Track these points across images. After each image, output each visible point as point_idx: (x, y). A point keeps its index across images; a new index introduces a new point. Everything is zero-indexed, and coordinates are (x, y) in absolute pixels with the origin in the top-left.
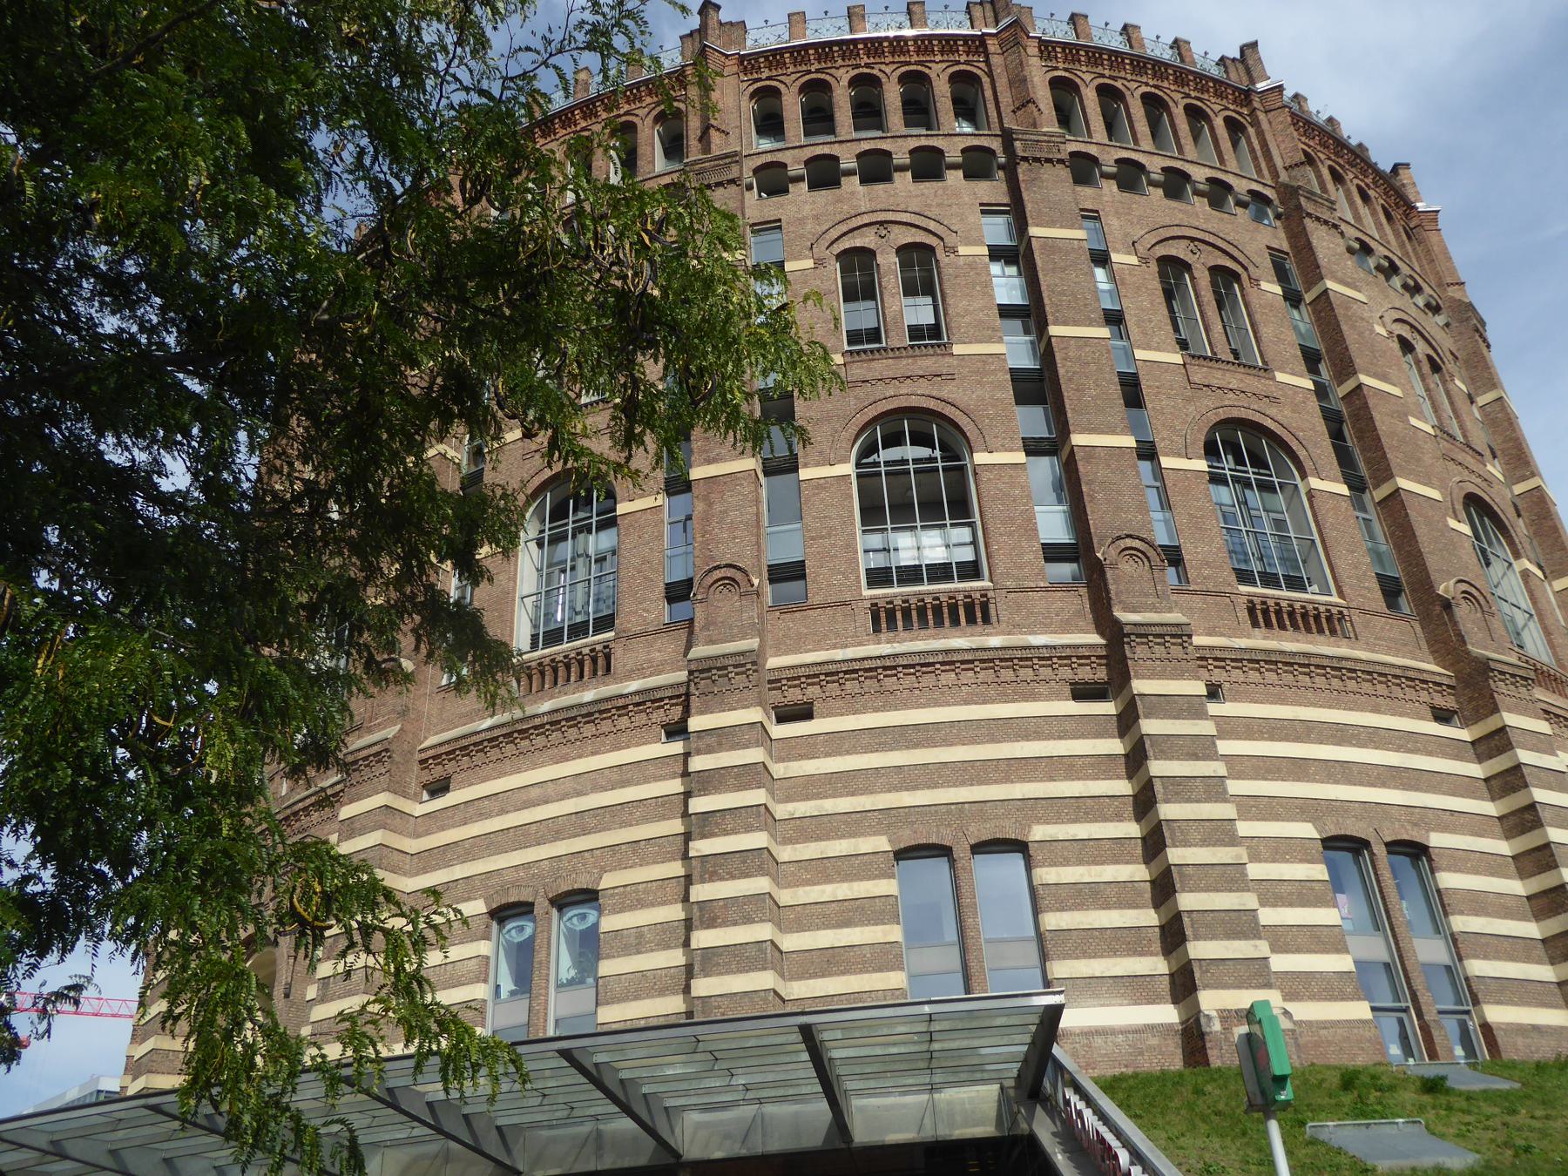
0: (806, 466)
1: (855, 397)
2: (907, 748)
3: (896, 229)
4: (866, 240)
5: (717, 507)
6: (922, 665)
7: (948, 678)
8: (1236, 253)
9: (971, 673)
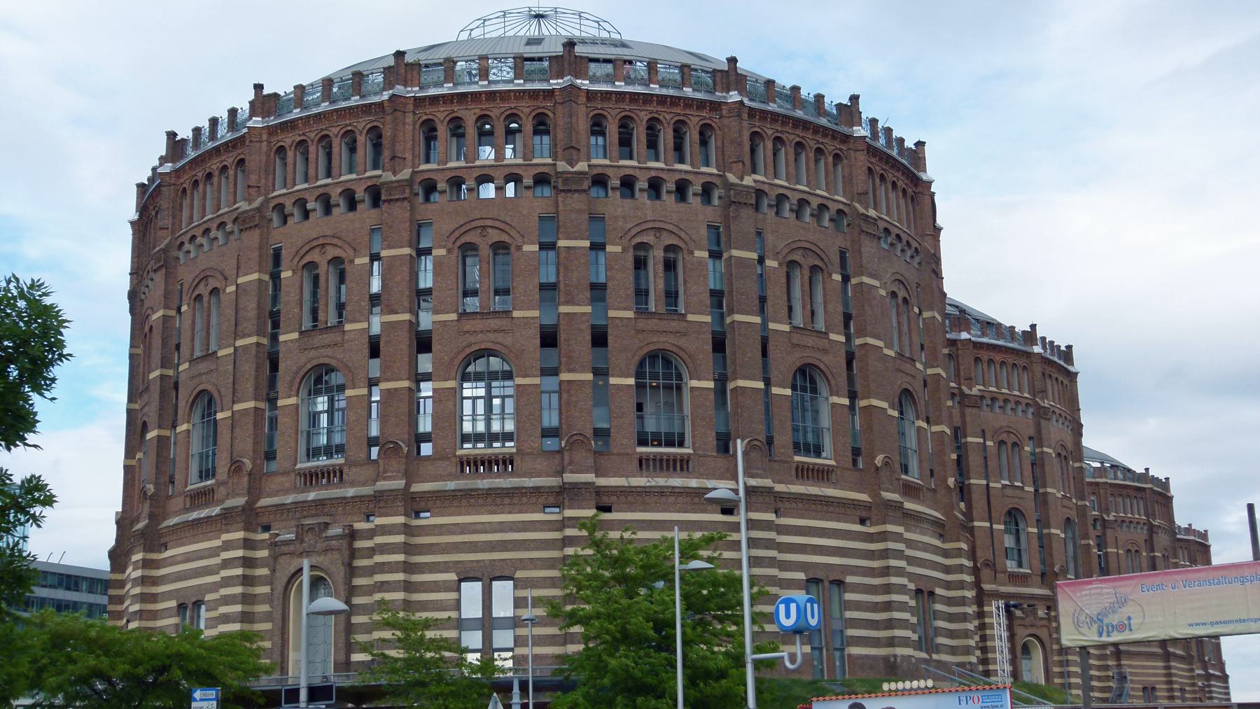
0: (613, 376)
1: (639, 339)
2: (653, 530)
3: (665, 234)
4: (648, 238)
5: (574, 399)
6: (662, 492)
7: (672, 499)
8: (824, 257)
9: (681, 498)
